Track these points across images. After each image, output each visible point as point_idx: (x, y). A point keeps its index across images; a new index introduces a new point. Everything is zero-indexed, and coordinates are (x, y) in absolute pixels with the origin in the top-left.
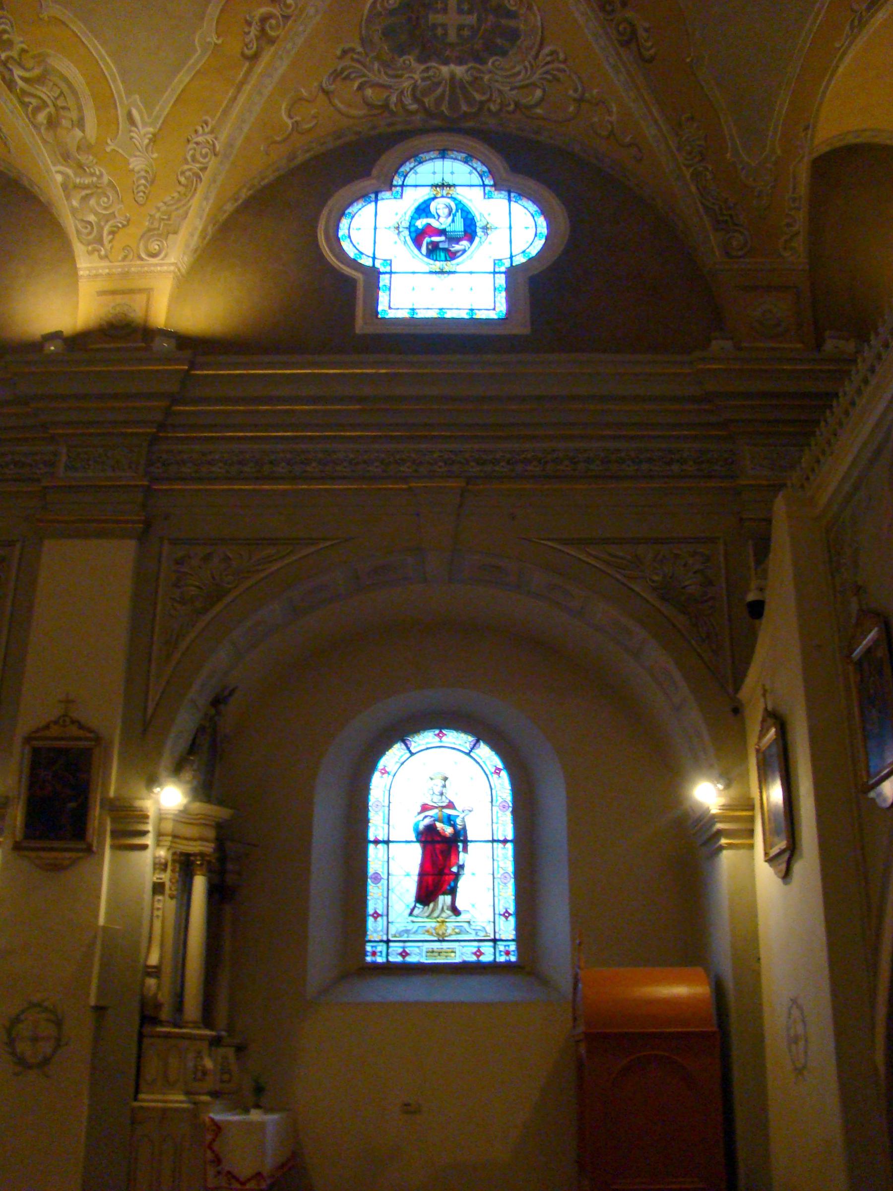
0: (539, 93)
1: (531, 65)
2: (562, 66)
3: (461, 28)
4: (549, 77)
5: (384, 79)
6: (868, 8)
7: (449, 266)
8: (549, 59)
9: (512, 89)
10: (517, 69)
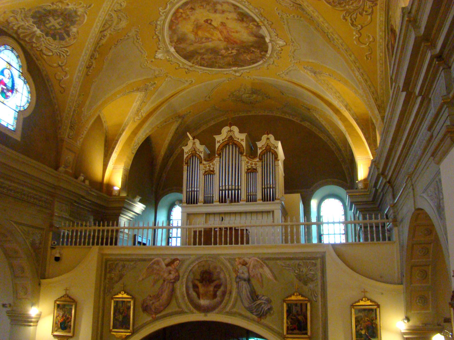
0: (51, 54)
1: (58, 47)
2: (65, 56)
3: (54, 26)
4: (59, 54)
5: (19, 19)
6: (128, 92)
7: (6, 101)
8: (64, 51)
9: (45, 47)
10: (53, 45)
